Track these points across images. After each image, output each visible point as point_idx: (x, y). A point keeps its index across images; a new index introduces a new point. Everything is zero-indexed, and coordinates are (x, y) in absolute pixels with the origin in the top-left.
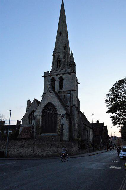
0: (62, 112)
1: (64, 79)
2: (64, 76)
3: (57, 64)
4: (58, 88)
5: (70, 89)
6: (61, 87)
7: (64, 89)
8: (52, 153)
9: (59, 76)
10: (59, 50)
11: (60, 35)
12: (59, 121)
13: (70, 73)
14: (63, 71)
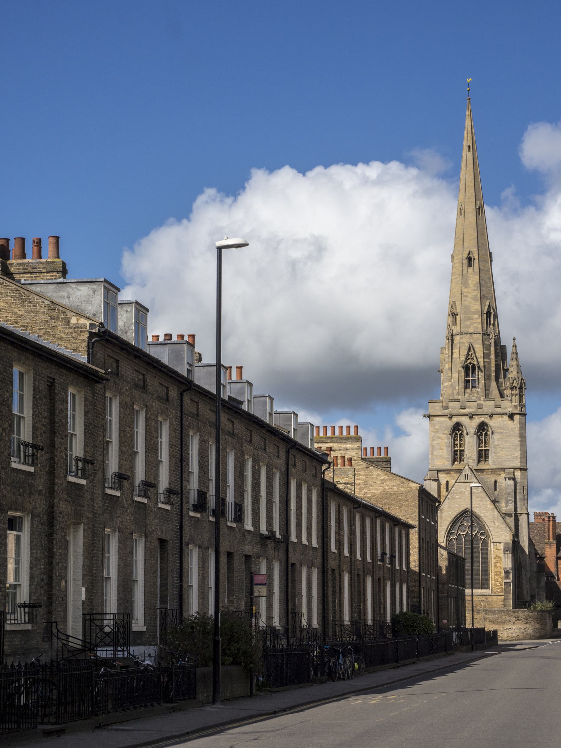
0: (503, 537)
1: (493, 433)
2: (493, 423)
3: (467, 375)
4: (475, 457)
5: (512, 465)
6: (483, 455)
7: (492, 463)
8: (518, 634)
9: (477, 421)
10: (468, 323)
11: (470, 265)
12: (495, 558)
13: (511, 416)
14: (488, 407)
